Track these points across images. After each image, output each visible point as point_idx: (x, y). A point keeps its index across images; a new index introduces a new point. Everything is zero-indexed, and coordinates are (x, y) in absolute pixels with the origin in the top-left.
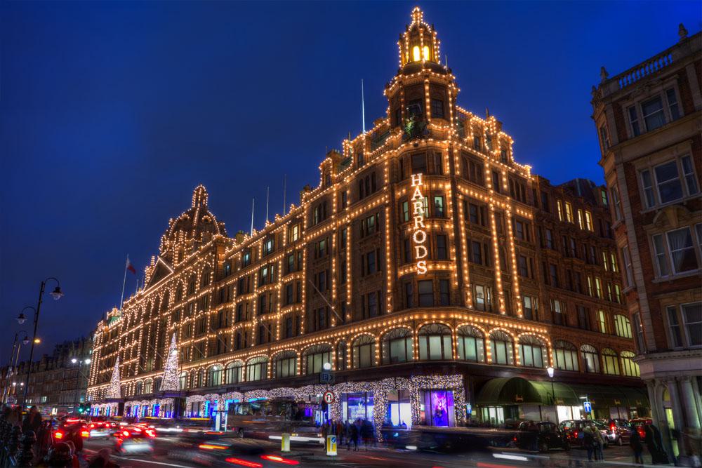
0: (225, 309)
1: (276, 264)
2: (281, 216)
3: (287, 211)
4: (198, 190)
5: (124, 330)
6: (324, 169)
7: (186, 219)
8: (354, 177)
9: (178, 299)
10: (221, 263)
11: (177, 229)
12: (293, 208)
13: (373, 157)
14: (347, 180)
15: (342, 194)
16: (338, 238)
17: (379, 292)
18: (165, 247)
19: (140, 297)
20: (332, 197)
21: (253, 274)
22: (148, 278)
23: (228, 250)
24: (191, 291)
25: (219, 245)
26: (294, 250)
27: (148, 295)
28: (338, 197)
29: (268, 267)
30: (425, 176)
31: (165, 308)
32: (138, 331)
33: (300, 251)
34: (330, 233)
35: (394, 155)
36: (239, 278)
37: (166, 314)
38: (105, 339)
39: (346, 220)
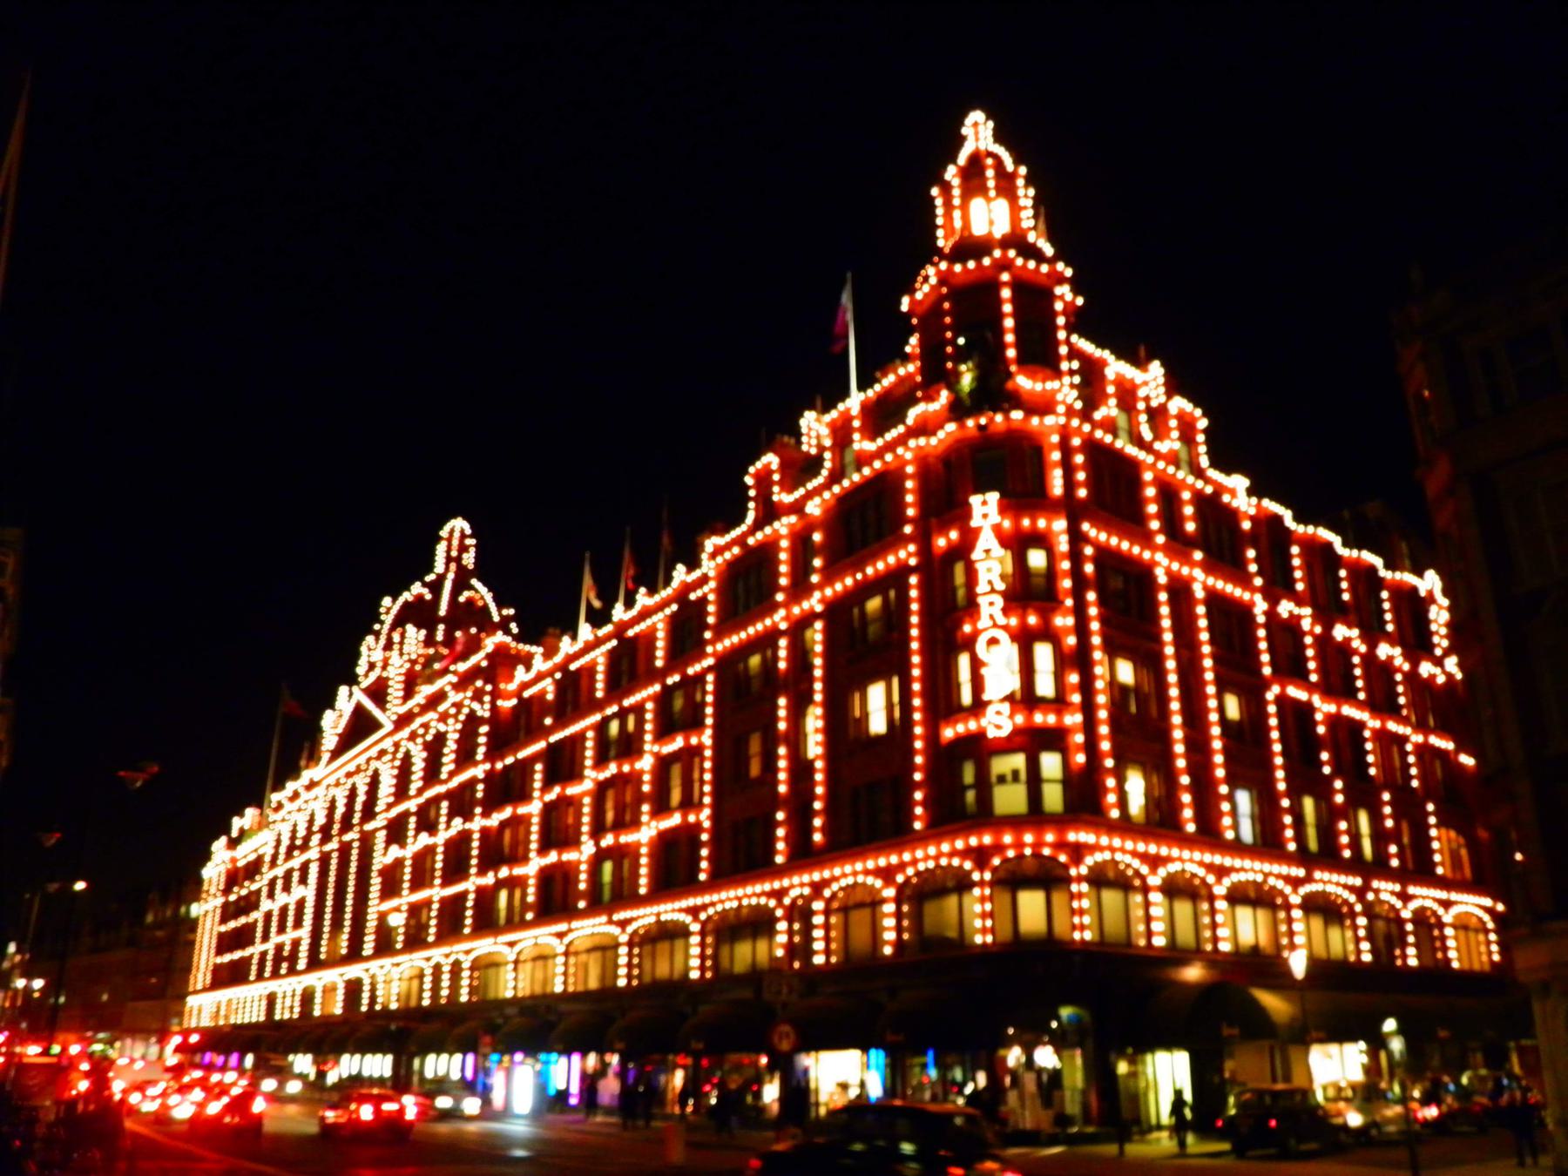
2: (652, 591)
3: (668, 581)
6: (758, 486)
9: (401, 793)
11: (399, 622)
12: (680, 574)
13: (879, 454)
14: (814, 508)
15: (801, 540)
19: (311, 785)
23: (521, 674)
25: (503, 662)
26: (685, 677)
30: (1005, 501)
31: (369, 813)
33: (700, 678)
34: (772, 635)
38: (234, 878)
39: (814, 603)
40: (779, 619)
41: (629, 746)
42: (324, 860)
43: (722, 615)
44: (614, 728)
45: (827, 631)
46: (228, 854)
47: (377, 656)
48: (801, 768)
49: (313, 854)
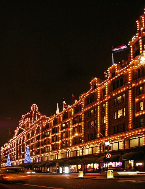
0: (47, 139)
1: (69, 122)
2: (70, 106)
3: (74, 103)
4: (34, 106)
5: (10, 148)
7: (29, 114)
8: (110, 82)
9: (28, 138)
10: (44, 125)
12: (76, 102)
16: (100, 108)
17: (124, 124)
18: (21, 123)
19: (14, 139)
20: (98, 93)
21: (59, 127)
22: (16, 134)
23: (47, 121)
24: (33, 135)
25: (44, 119)
27: (17, 138)
28: (101, 92)
29: (65, 123)
31: (23, 141)
32: (15, 148)
35: (135, 68)
36: (52, 129)
37: (24, 143)
38: (4, 151)
40: (98, 103)
41: (67, 126)
42: (17, 148)
43: (85, 106)
44: (64, 125)
45: (109, 104)
46: (3, 149)
47: (22, 122)
48: (103, 125)
49: (16, 147)
